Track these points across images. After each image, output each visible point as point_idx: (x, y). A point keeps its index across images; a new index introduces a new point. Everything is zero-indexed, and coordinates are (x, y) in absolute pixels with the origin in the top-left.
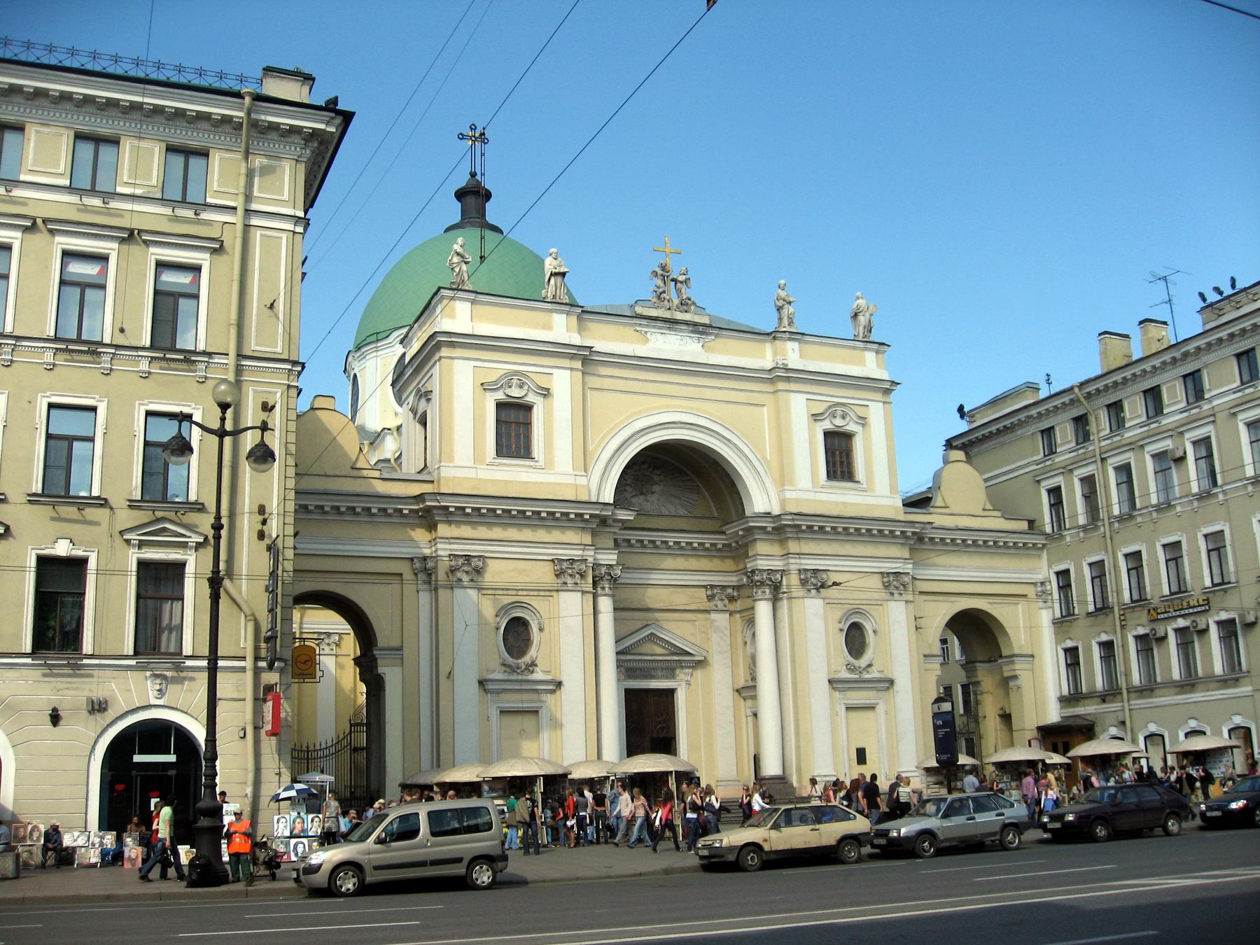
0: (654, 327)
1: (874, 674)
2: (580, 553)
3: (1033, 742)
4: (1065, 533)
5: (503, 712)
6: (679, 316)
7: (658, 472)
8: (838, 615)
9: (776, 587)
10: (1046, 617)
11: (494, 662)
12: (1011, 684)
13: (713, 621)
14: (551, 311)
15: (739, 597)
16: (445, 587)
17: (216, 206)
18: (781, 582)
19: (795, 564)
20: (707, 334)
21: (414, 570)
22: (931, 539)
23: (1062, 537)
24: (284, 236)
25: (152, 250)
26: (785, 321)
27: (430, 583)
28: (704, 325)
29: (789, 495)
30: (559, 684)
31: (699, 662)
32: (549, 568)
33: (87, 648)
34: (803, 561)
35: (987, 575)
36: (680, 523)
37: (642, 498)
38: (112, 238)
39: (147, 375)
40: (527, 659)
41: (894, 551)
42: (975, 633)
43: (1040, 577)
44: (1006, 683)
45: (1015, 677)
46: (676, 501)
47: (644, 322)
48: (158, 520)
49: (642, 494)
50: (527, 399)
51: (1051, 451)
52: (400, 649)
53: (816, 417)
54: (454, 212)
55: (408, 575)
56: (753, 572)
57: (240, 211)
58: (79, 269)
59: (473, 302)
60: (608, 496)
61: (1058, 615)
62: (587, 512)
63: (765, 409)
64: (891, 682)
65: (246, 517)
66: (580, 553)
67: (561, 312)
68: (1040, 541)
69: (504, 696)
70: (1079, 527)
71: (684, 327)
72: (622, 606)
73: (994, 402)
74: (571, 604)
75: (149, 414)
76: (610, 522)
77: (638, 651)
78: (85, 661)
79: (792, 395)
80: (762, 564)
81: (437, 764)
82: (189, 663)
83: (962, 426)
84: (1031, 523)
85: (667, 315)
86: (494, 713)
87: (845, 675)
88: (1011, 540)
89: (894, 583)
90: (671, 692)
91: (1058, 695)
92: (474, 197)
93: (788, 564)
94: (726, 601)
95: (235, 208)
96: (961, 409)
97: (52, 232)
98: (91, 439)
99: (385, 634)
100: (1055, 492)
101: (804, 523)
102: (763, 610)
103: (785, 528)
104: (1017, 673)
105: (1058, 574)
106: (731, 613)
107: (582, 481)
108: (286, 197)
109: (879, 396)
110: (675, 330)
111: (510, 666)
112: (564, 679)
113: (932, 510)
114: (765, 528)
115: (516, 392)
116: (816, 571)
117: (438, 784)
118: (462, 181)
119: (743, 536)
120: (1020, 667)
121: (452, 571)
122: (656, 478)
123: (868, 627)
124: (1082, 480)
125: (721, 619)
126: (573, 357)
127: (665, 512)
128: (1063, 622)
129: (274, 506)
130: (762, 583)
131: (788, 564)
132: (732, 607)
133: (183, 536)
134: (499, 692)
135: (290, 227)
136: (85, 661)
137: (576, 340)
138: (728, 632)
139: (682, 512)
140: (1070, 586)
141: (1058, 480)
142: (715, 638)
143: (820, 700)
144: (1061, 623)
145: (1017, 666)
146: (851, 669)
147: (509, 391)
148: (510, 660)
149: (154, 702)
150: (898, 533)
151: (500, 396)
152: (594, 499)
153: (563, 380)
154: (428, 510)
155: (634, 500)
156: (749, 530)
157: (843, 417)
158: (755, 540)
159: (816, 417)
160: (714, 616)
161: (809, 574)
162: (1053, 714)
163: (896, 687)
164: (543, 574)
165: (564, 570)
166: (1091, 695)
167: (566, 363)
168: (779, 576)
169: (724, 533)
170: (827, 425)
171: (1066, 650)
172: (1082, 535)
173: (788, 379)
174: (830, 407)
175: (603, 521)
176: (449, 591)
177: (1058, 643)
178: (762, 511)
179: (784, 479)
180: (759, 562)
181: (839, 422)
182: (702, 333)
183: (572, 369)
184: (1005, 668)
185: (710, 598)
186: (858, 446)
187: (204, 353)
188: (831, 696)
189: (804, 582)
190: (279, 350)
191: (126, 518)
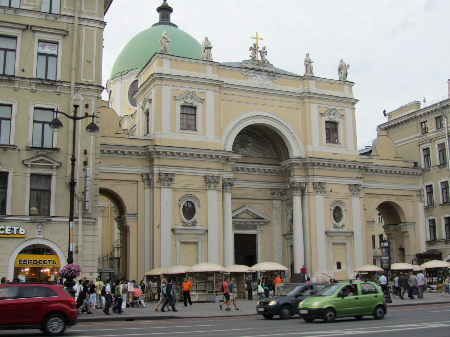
0: (251, 73)
1: (345, 229)
2: (217, 173)
3: (414, 262)
4: (431, 169)
5: (181, 243)
6: (262, 68)
7: (250, 137)
9: (303, 191)
10: (421, 206)
11: (178, 221)
12: (405, 235)
13: (273, 204)
14: (206, 65)
15: (285, 194)
16: (157, 187)
17: (65, 16)
18: (305, 188)
19: (311, 180)
20: (274, 76)
21: (143, 179)
22: (371, 170)
23: (429, 170)
24: (96, 30)
25: (37, 34)
26: (309, 71)
27: (150, 185)
28: (273, 72)
29: (309, 149)
30: (207, 231)
31: (267, 222)
32: (202, 179)
33: (8, 212)
34: (315, 179)
35: (396, 187)
36: (260, 161)
37: (243, 149)
38: (19, 29)
39: (34, 91)
40: (193, 220)
42: (390, 212)
43: (419, 188)
44: (403, 235)
45: (407, 232)
46: (258, 151)
47: (246, 70)
48: (40, 156)
49: (243, 147)
50: (194, 104)
51: (425, 131)
52: (136, 214)
53: (322, 115)
54: (156, 17)
55: (140, 182)
56: (293, 183)
57: (76, 18)
58: (47, 50)
59: (171, 60)
60: (229, 148)
61: (426, 205)
62: (220, 155)
63: (299, 110)
64: (353, 233)
65: (79, 155)
66: (217, 173)
67: (211, 65)
68: (419, 172)
69: (183, 236)
70: (437, 166)
71: (264, 73)
72: (234, 197)
73: (401, 109)
74: (213, 196)
75: (36, 108)
76: (230, 159)
77: (241, 217)
78: (8, 218)
79: (311, 104)
80: (297, 179)
81: (152, 267)
82: (53, 219)
83: (385, 120)
84: (416, 164)
85: (257, 67)
86: (178, 244)
87: (332, 229)
88: (407, 170)
89: (355, 189)
90: (254, 236)
91: (425, 240)
92: (165, 11)
93: (308, 180)
94: (279, 195)
95: (74, 17)
96: (384, 112)
97: (34, 31)
98: (10, 119)
99: (130, 206)
100: (427, 150)
101: (316, 162)
102: (297, 200)
103: (307, 164)
104: (408, 230)
105: (427, 186)
106: (282, 201)
107: (218, 141)
108: (96, 12)
109: (350, 106)
110: (260, 74)
111: (185, 223)
112: (209, 229)
113: (372, 157)
115: (189, 101)
116: (320, 183)
117: (165, 276)
118: (160, 3)
119: (289, 167)
120: (409, 228)
121: (160, 180)
122: (250, 140)
123: (343, 209)
124: (439, 145)
125: (277, 203)
126: (215, 85)
127: (253, 155)
128: (429, 208)
129: (91, 151)
130: (297, 188)
131: (308, 180)
132: (282, 198)
133: (50, 163)
134: (180, 234)
135: (98, 26)
136: (8, 218)
137: (216, 77)
138: (280, 209)
139: (261, 155)
140: (432, 192)
141: (428, 145)
142: (274, 212)
143: (320, 240)
144: (428, 208)
145: (408, 227)
146: (335, 227)
147: (186, 100)
148: (186, 220)
149: (38, 236)
150: (357, 167)
151: (182, 103)
152: (223, 149)
153: (210, 96)
154: (150, 153)
155: (240, 150)
156: (292, 164)
157: (334, 115)
158: (294, 169)
159: (322, 115)
160: (274, 202)
161: (317, 184)
162: (423, 249)
164: (200, 182)
165: (210, 181)
166: (440, 241)
167: (211, 88)
168: (304, 185)
169: (280, 165)
170: (327, 118)
171: (429, 220)
172: (438, 169)
173: (310, 97)
174: (328, 110)
175: (227, 160)
176: (159, 189)
177: (426, 216)
178: (297, 156)
179: (306, 142)
180: (295, 179)
181: (332, 117)
182: (272, 76)
183: (215, 91)
184: (402, 228)
185: (272, 194)
186: (340, 128)
187: (60, 82)
188: (326, 239)
189: (315, 188)
190: (93, 81)
191: (25, 155)
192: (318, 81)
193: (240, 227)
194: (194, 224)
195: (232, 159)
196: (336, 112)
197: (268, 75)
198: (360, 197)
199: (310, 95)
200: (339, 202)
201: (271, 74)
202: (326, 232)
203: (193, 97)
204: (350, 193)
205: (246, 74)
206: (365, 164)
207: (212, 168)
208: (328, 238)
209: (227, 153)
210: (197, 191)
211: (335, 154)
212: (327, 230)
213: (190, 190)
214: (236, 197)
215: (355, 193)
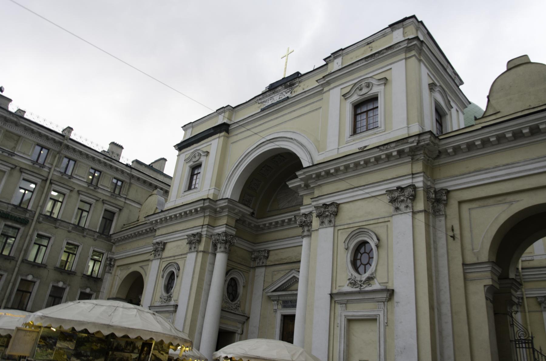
0: (267, 96)
1: (376, 286)
8: (343, 236)
41: (406, 169)
62: (199, 206)
66: (199, 231)
71: (280, 88)
87: (347, 289)
89: (399, 198)
110: (277, 92)
114: (300, 186)
146: (353, 283)
147: (194, 160)
157: (368, 87)
163: (396, 298)
170: (355, 98)
181: (365, 90)
189: (318, 216)
192: (347, 54)
193: (290, 304)
194: (169, 298)
195: (222, 208)
196: (370, 80)
197: (285, 88)
198: (414, 213)
199: (327, 80)
200: (361, 231)
201: (288, 83)
202: (332, 295)
203: (199, 153)
204: (391, 209)
205: (263, 100)
206: (410, 140)
207: (196, 224)
208: (338, 307)
209: (202, 202)
210: (180, 257)
211: (365, 147)
212: (335, 291)
213: (176, 258)
214: (289, 261)
215: (402, 206)
